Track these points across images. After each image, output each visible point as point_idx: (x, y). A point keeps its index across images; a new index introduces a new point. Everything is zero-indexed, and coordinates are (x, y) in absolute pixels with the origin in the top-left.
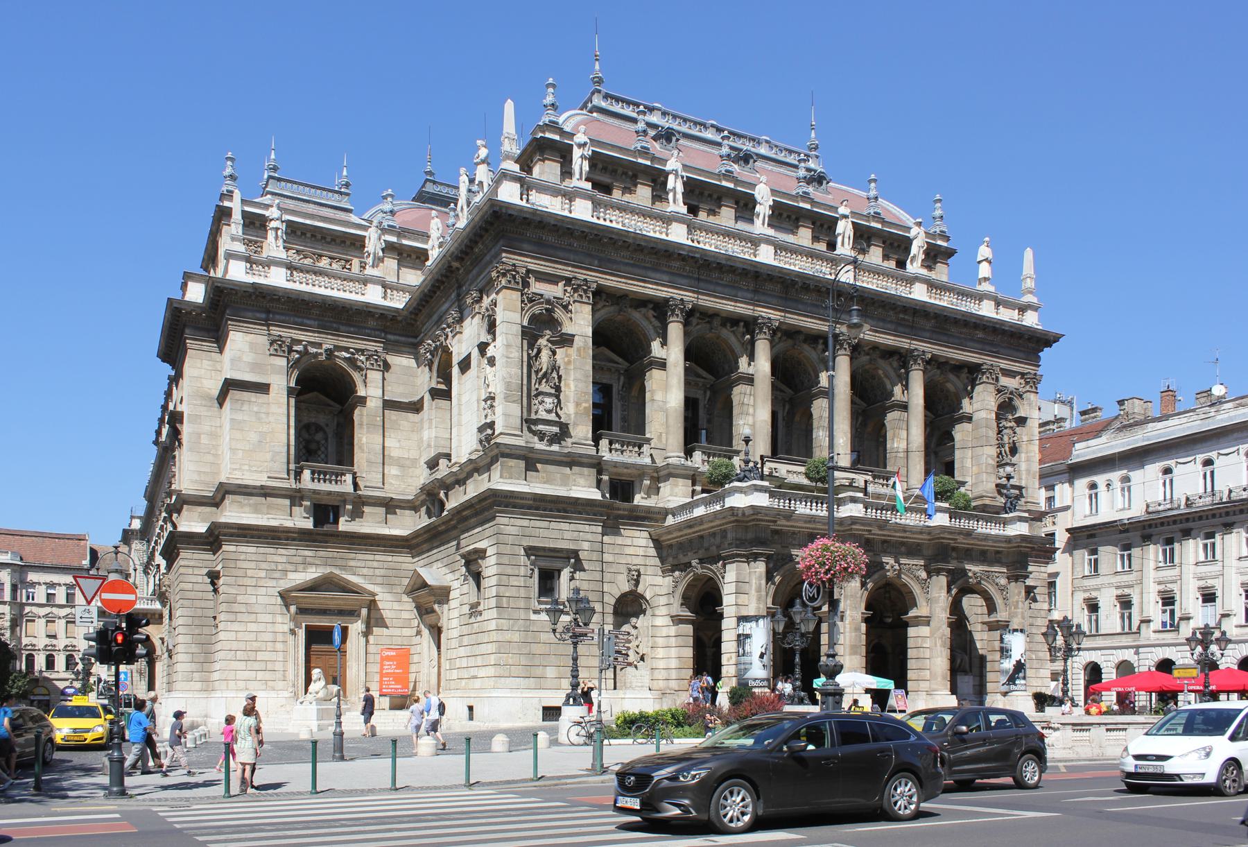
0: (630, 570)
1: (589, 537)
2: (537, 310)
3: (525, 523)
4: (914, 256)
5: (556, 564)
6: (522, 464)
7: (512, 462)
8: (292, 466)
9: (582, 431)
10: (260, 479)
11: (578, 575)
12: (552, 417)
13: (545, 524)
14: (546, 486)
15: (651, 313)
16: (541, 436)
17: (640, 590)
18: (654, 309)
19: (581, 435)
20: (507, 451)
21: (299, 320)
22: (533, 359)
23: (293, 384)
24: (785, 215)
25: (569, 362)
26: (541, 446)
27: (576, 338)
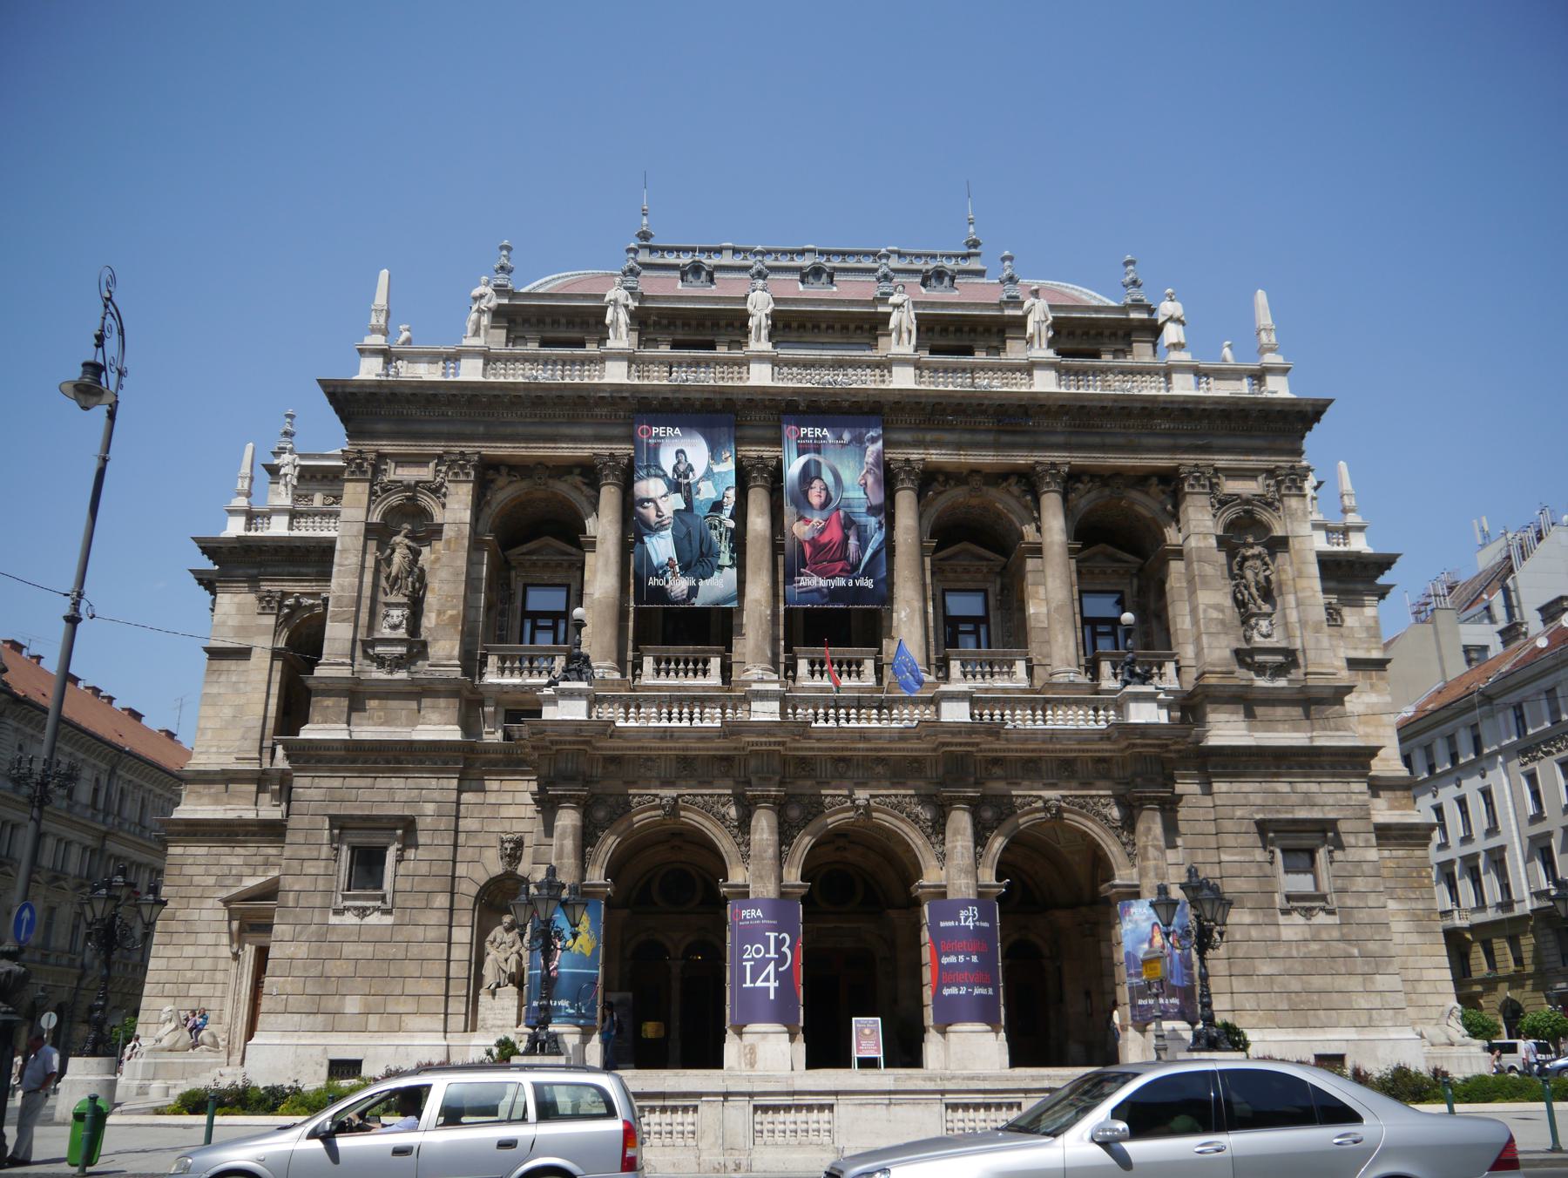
0: (503, 842)
1: (436, 795)
2: (395, 500)
3: (337, 783)
4: (1032, 337)
5: (377, 839)
6: (345, 702)
7: (329, 702)
8: (268, 743)
9: (445, 650)
10: (229, 763)
11: (410, 854)
12: (401, 633)
13: (369, 781)
14: (382, 728)
15: (578, 479)
16: (380, 661)
17: (523, 868)
18: (581, 474)
19: (441, 653)
20: (322, 686)
21: (292, 569)
22: (384, 562)
23: (281, 644)
24: (852, 326)
25: (438, 559)
26: (381, 675)
27: (446, 527)
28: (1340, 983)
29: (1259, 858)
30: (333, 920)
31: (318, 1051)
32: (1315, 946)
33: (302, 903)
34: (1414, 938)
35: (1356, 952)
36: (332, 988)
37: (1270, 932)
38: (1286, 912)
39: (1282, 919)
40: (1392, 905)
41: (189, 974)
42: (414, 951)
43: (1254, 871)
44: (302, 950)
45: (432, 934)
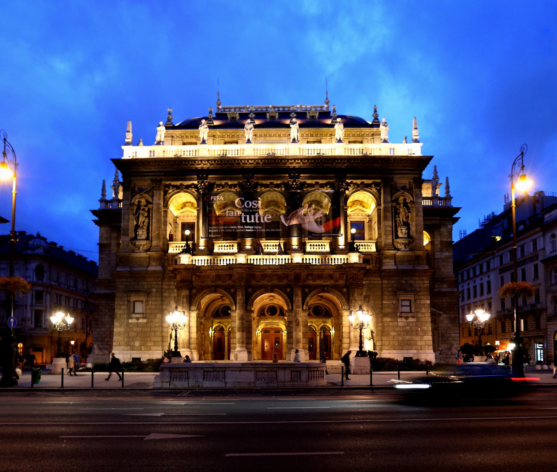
28: (414, 338)
29: (394, 302)
30: (130, 321)
31: (129, 356)
32: (408, 328)
33: (122, 317)
34: (450, 325)
35: (420, 329)
36: (131, 339)
37: (395, 324)
38: (401, 317)
39: (399, 320)
40: (445, 316)
41: (104, 336)
42: (152, 329)
43: (392, 306)
44: (122, 330)
45: (157, 325)
